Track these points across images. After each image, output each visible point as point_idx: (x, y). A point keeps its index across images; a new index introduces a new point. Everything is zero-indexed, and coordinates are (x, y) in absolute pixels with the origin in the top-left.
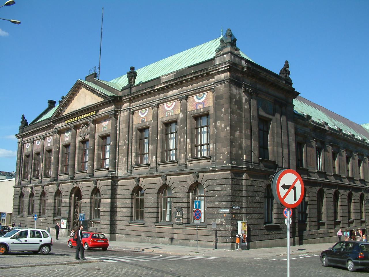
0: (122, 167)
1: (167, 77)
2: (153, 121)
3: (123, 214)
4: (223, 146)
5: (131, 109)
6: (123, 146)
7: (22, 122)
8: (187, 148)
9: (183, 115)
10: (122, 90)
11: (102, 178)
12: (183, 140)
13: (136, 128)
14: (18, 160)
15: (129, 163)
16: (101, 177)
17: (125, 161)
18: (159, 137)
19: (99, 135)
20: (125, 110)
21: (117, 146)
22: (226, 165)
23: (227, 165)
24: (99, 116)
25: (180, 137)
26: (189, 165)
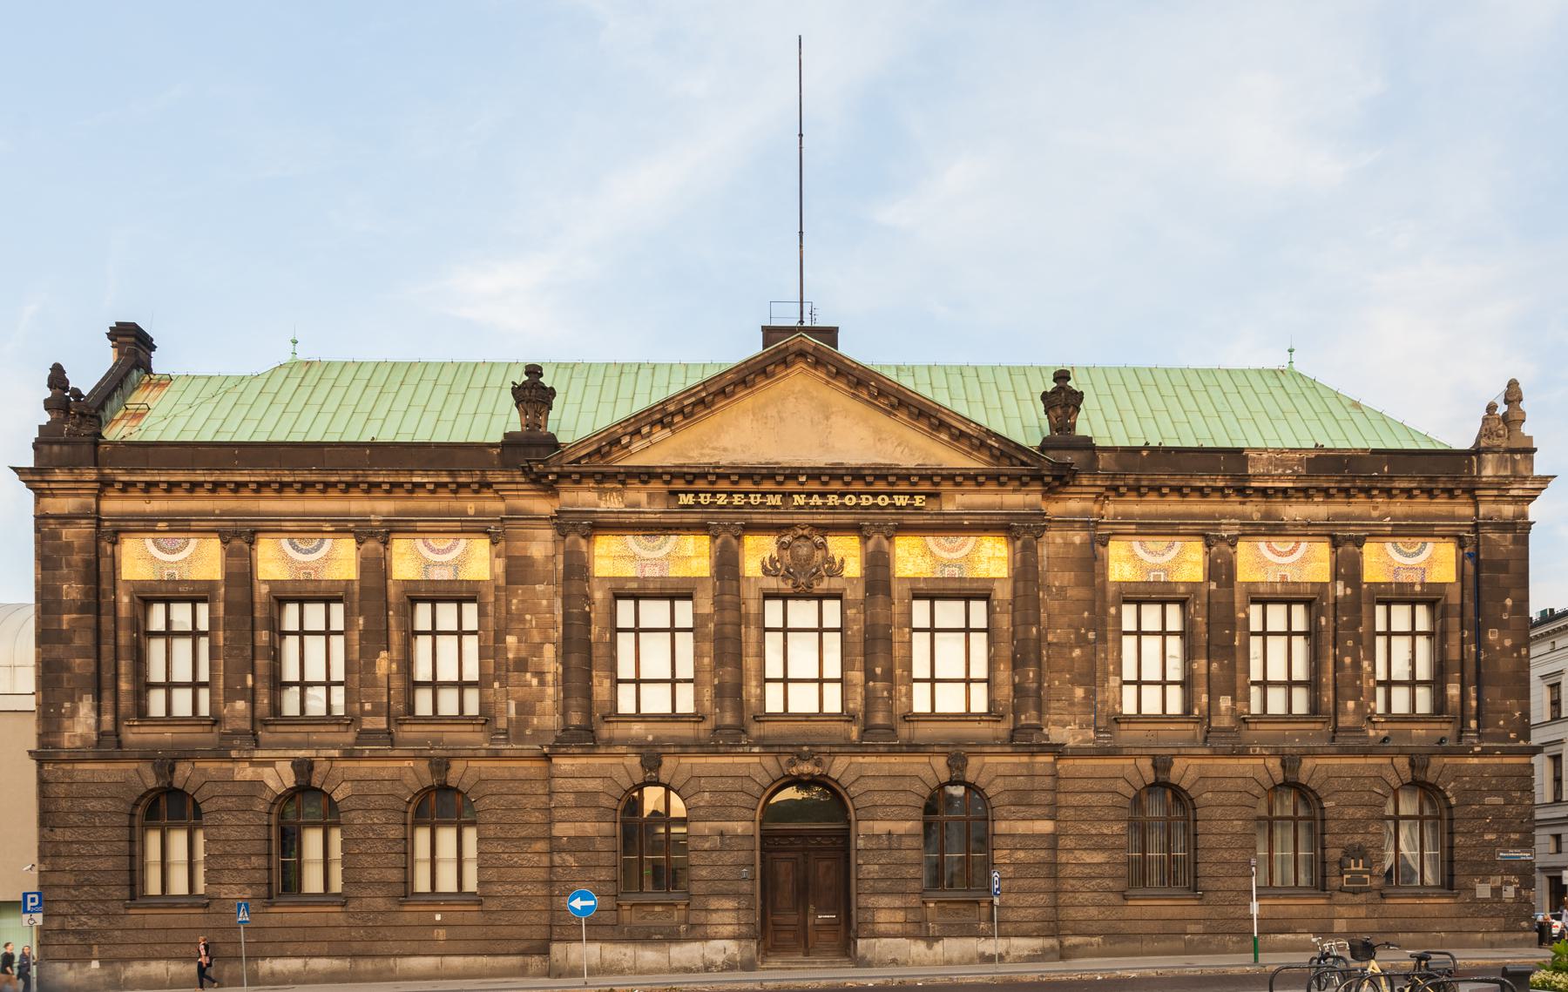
0: (1067, 718)
1: (1277, 459)
2: (1213, 586)
3: (1088, 871)
4: (1506, 696)
5: (1100, 527)
6: (1072, 648)
8: (1365, 686)
9: (1349, 591)
10: (1042, 448)
12: (1352, 662)
13: (1121, 593)
18: (1240, 641)
19: (912, 589)
20: (1078, 525)
22: (1516, 744)
23: (1522, 743)
25: (1476, 647)
26: (1372, 733)
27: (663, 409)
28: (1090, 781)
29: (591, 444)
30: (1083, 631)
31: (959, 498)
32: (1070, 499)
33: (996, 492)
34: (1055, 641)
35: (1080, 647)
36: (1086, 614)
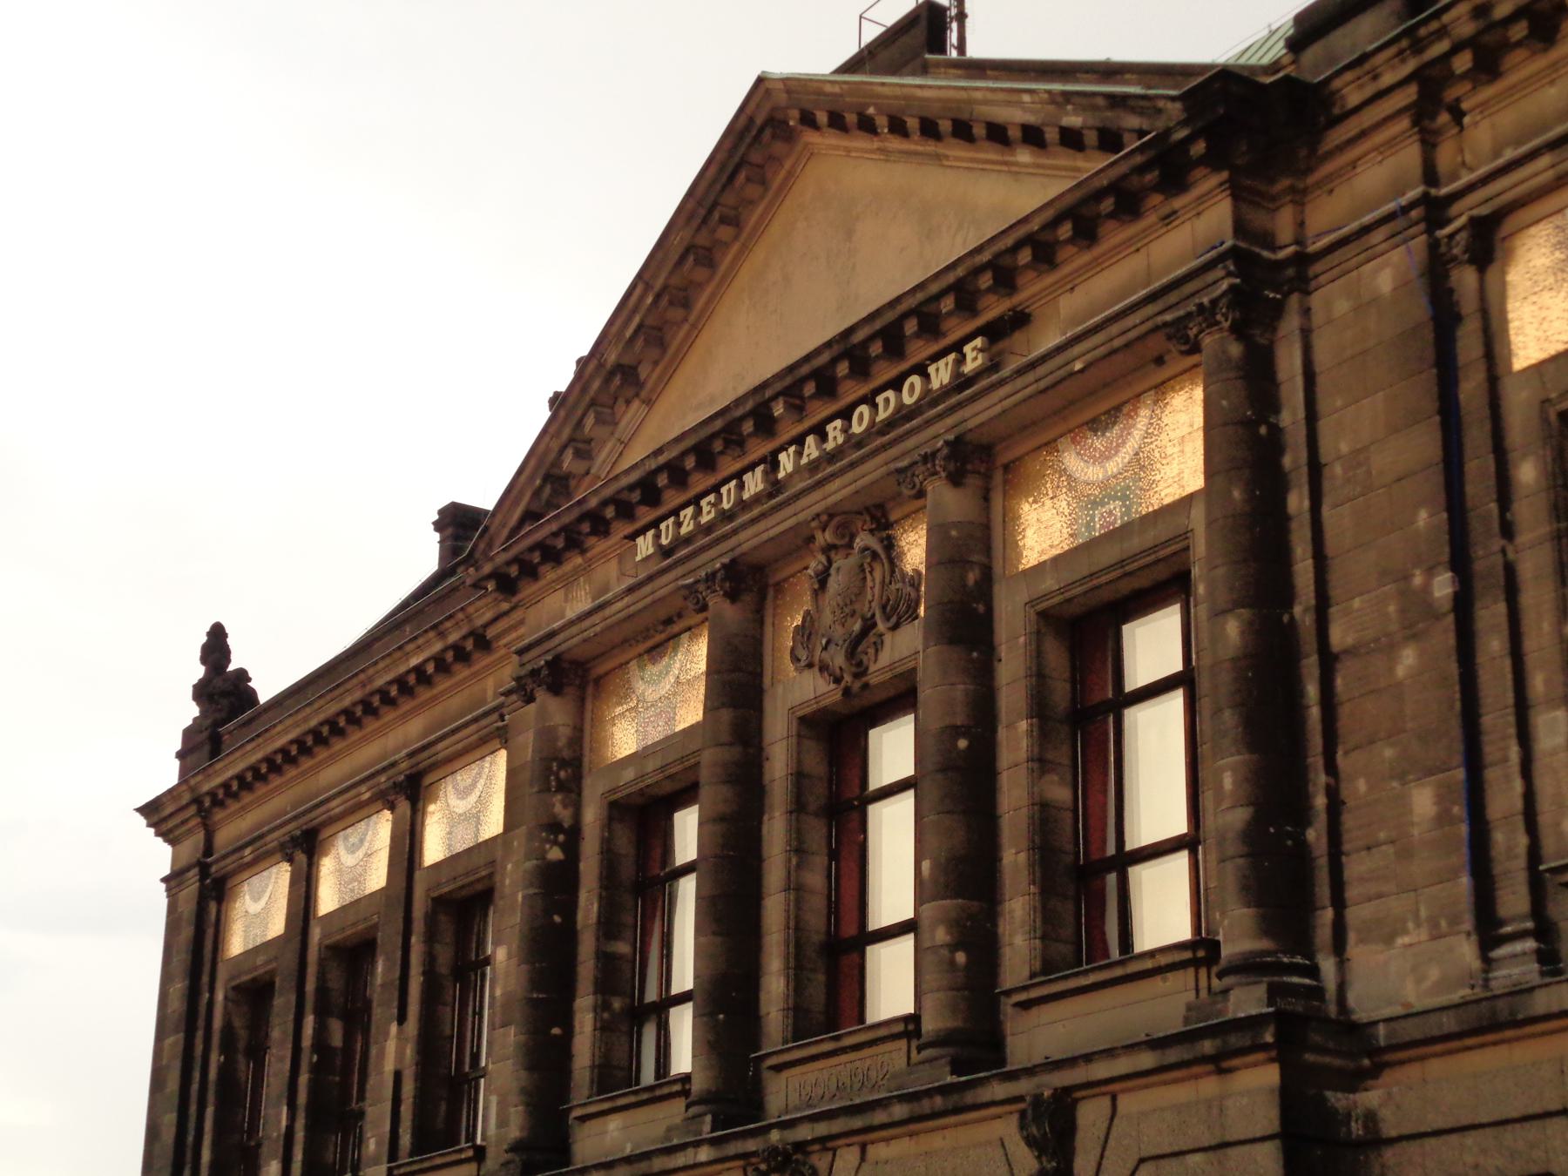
0: (1396, 905)
5: (1455, 208)
6: (1390, 649)
7: (202, 692)
11: (1147, 1060)
13: (1546, 401)
14: (170, 1040)
15: (1509, 842)
16: (1132, 1048)
17: (1443, 818)
19: (1031, 603)
20: (1378, 236)
21: (1310, 666)
24: (1041, 370)
27: (601, 365)
28: (1470, 1139)
29: (521, 493)
30: (1418, 580)
31: (1068, 304)
32: (1353, 165)
33: (1133, 246)
34: (1350, 640)
35: (1415, 637)
36: (1423, 515)
